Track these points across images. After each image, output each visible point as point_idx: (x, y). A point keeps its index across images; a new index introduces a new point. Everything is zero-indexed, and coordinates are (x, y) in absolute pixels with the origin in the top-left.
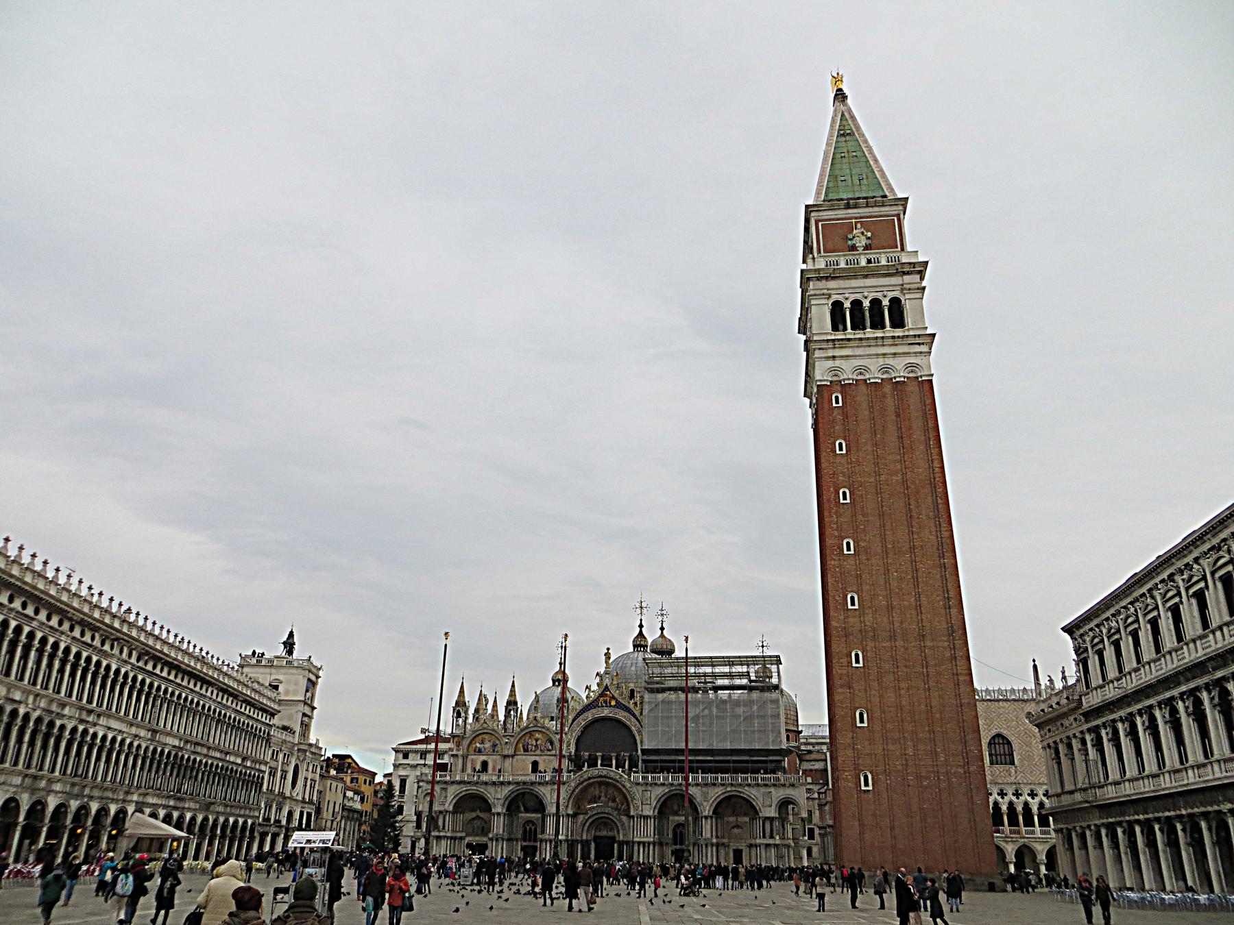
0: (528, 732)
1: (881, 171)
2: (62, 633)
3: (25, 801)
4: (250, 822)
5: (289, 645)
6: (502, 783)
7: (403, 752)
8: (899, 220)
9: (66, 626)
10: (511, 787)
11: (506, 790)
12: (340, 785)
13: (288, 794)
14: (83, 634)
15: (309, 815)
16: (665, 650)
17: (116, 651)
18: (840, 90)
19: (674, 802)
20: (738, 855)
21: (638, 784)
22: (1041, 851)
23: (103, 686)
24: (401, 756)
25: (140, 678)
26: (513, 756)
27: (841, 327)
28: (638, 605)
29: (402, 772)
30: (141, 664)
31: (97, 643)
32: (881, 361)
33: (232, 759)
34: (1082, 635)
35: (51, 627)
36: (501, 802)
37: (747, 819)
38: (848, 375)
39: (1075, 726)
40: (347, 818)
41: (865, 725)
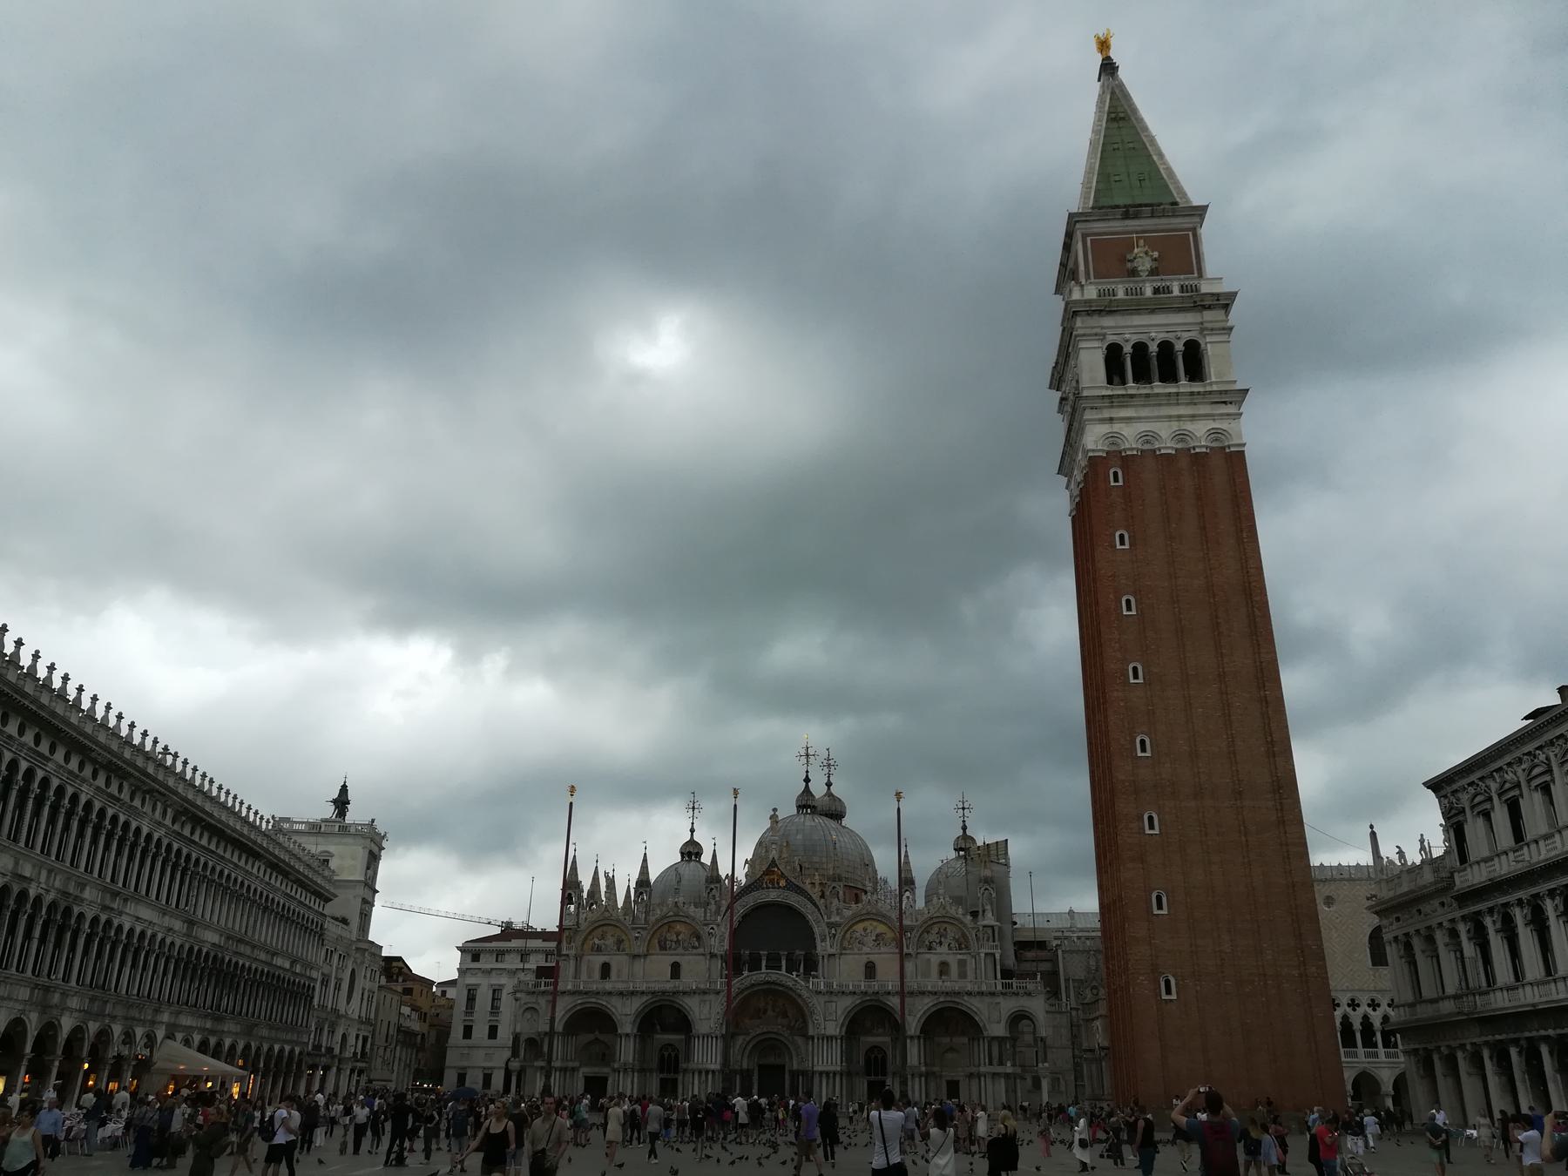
0: (667, 923)
1: (1169, 169)
2: (84, 781)
4: (297, 1050)
5: (341, 803)
6: (633, 993)
7: (472, 952)
8: (1195, 236)
9: (88, 771)
10: (645, 998)
13: (342, 1012)
14: (108, 784)
16: (835, 813)
17: (147, 808)
18: (1109, 58)
22: (1386, 1077)
24: (469, 957)
26: (645, 956)
27: (1116, 379)
28: (803, 752)
29: (471, 980)
30: (177, 827)
31: (125, 796)
32: (1175, 426)
33: (279, 961)
34: (1454, 792)
35: (71, 772)
36: (631, 1018)
37: (965, 1040)
39: (1439, 914)
41: (1165, 912)
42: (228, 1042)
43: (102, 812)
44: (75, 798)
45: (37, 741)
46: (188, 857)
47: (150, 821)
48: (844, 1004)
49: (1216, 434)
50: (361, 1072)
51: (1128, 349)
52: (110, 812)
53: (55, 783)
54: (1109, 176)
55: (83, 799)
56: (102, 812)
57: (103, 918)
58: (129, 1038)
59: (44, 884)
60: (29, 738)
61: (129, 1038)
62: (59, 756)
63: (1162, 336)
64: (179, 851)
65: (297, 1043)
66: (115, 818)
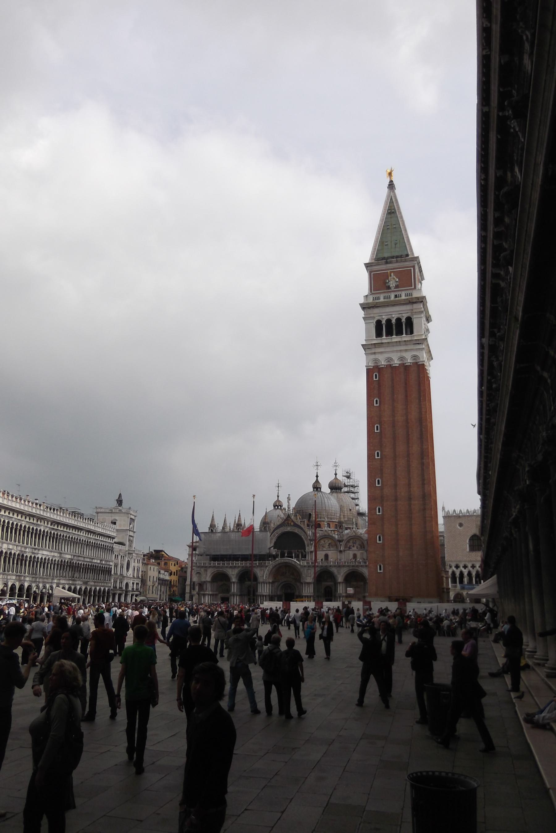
3: (17, 585)
4: (107, 589)
5: (120, 502)
6: (235, 567)
8: (414, 269)
9: (24, 517)
12: (156, 568)
17: (42, 523)
18: (391, 181)
21: (305, 566)
23: (39, 539)
25: (53, 532)
31: (35, 522)
32: (399, 354)
33: (95, 561)
37: (362, 583)
42: (78, 587)
43: (29, 528)
44: (21, 526)
45: (9, 513)
46: (57, 534)
47: (43, 527)
50: (137, 596)
51: (384, 322)
52: (31, 527)
53: (15, 523)
54: (383, 243)
55: (23, 526)
56: (29, 528)
57: (33, 556)
59: (16, 550)
60: (7, 514)
61: (45, 587)
64: (54, 533)
65: (106, 587)
66: (33, 528)
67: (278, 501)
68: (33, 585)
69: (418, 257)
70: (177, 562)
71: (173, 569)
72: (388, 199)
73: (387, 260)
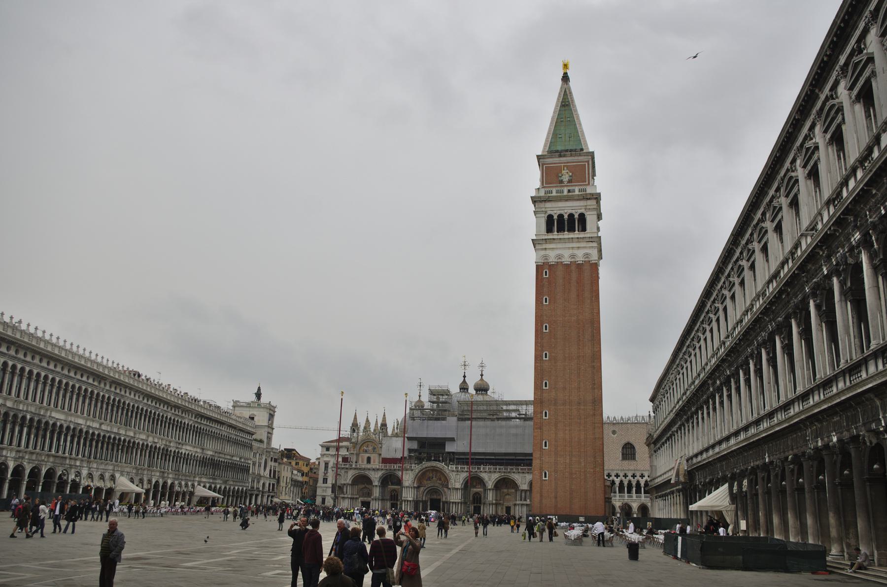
1: (582, 131)
3: (161, 482)
5: (258, 395)
11: (380, 474)
15: (273, 485)
16: (482, 389)
19: (474, 481)
20: (508, 509)
29: (326, 459)
32: (571, 251)
33: (235, 458)
38: (552, 259)
40: (294, 486)
42: (218, 486)
47: (188, 420)
48: (464, 475)
49: (587, 255)
50: (272, 497)
51: (555, 217)
58: (186, 485)
59: (160, 444)
60: (154, 404)
61: (186, 485)
62: (162, 406)
63: (570, 211)
67: (420, 401)
68: (176, 482)
69: (593, 153)
70: (307, 460)
71: (306, 469)
72: (561, 91)
73: (561, 154)
